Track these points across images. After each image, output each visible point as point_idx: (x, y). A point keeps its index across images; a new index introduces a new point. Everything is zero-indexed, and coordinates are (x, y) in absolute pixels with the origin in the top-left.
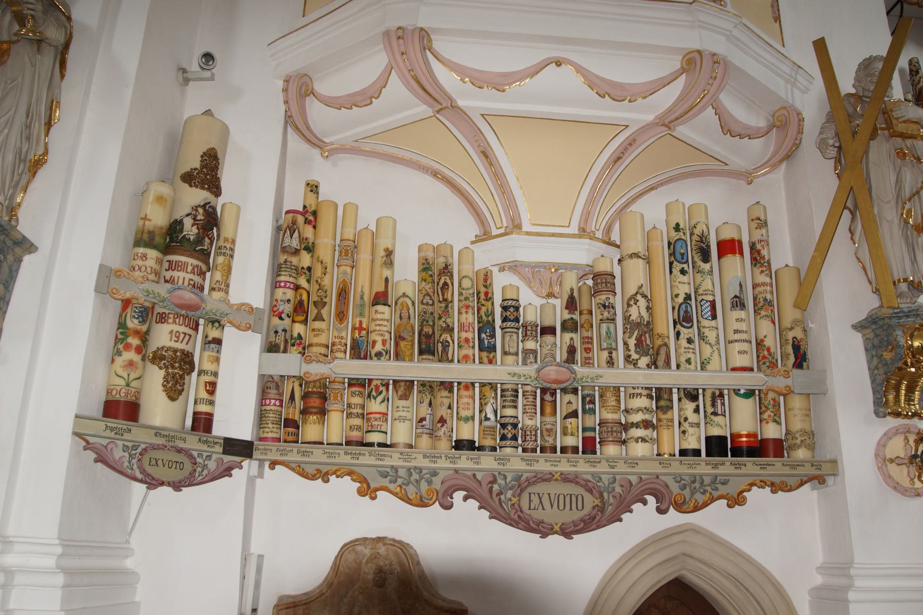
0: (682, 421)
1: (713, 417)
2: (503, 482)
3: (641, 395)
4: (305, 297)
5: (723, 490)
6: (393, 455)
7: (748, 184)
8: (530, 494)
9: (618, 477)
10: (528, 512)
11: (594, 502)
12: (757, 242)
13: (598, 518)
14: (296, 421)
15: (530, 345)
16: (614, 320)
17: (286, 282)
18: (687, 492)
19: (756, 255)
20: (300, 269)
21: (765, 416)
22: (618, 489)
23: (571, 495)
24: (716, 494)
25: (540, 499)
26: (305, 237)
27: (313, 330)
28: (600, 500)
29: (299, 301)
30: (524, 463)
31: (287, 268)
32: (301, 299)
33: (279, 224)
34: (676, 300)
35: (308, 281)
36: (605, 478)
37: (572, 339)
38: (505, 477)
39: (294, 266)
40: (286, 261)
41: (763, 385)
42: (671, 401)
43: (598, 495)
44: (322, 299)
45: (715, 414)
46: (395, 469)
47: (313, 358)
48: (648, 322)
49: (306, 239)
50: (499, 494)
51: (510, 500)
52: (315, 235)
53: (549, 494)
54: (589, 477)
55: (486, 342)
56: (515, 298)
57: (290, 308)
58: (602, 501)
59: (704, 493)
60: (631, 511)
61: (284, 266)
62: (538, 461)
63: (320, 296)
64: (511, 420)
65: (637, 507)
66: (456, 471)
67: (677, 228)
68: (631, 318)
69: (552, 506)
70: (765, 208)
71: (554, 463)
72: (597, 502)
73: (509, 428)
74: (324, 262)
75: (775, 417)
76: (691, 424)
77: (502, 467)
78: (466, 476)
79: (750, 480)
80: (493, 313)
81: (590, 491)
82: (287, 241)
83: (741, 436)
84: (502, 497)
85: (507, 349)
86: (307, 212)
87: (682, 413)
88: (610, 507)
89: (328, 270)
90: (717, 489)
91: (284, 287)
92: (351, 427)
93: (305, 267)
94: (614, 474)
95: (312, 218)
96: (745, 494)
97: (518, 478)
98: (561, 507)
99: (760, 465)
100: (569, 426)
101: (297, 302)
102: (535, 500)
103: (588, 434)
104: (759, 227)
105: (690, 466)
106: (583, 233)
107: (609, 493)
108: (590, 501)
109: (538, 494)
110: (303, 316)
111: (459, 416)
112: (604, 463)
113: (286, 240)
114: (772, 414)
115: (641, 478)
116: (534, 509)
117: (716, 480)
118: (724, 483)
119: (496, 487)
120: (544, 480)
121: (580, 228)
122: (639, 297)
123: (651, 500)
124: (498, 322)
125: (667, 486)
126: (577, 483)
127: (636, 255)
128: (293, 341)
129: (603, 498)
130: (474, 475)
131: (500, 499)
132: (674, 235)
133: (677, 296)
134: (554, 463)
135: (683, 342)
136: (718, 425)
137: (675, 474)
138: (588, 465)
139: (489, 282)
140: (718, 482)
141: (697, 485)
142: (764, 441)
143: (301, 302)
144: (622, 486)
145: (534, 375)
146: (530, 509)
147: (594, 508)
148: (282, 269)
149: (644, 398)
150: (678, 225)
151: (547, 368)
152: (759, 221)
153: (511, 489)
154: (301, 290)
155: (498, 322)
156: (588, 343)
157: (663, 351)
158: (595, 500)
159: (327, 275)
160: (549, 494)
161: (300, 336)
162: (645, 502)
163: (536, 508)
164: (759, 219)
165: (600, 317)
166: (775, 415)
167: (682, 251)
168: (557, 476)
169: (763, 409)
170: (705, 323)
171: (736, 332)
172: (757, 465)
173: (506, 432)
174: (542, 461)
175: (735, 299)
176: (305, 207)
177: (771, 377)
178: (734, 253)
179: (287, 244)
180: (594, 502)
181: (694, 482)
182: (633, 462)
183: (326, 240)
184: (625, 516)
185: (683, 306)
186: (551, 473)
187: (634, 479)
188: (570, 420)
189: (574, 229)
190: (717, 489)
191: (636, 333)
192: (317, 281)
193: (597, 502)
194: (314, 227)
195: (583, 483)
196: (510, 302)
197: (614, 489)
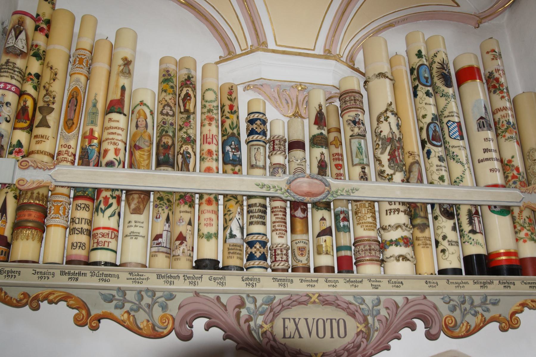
0: (440, 239)
1: (471, 235)
2: (252, 306)
3: (398, 210)
4: (30, 103)
5: (494, 311)
6: (121, 275)
7: (475, 28)
8: (284, 319)
9: (382, 298)
10: (283, 341)
11: (358, 327)
12: (494, 72)
13: (363, 346)
14: (6, 237)
15: (279, 159)
16: (364, 136)
17: (6, 84)
18: (457, 314)
19: (495, 83)
20: (26, 75)
21: (522, 234)
22: (384, 312)
23: (331, 320)
24: (488, 316)
25: (296, 325)
26: (35, 44)
27: (36, 137)
28: (364, 325)
29: (22, 107)
30: (277, 283)
31: (9, 69)
32: (25, 105)
33: (4, 26)
34: (424, 121)
35: (35, 88)
36: (369, 300)
37: (322, 154)
38: (255, 300)
39: (18, 68)
40: (8, 62)
41: (520, 202)
42: (427, 218)
43: (361, 319)
44: (49, 105)
45: (473, 232)
46: (123, 291)
47: (31, 163)
48: (399, 138)
49: (37, 46)
50: (247, 321)
51: (261, 327)
52: (47, 44)
53: (306, 319)
54: (351, 299)
55: (231, 154)
56: (261, 111)
57: (9, 111)
58: (367, 326)
59: (475, 314)
60: (399, 338)
61: (4, 67)
62: (292, 281)
63: (47, 102)
64: (260, 238)
65: (405, 332)
66: (197, 294)
67: (419, 54)
68: (382, 134)
69: (310, 333)
70: (497, 42)
71: (311, 284)
72: (361, 327)
73: (258, 246)
74: (53, 68)
75: (533, 236)
76: (451, 243)
77: (250, 288)
78: (208, 299)
79: (521, 300)
80: (238, 126)
81: (353, 315)
82: (11, 42)
83: (499, 255)
84: (252, 324)
85: (254, 162)
86: (39, 20)
87: (439, 232)
88: (376, 333)
89: (57, 76)
90: (488, 310)
91: (4, 88)
92: (73, 244)
93: (33, 73)
94: (378, 295)
95: (45, 26)
96: (517, 315)
97: (269, 301)
98: (321, 334)
99: (529, 283)
100: (324, 244)
101: (20, 107)
103: (343, 253)
104: (494, 58)
105: (458, 285)
106: (328, 55)
107: (374, 317)
109: (294, 319)
110: (26, 123)
111: (201, 233)
112: (366, 282)
113: (10, 41)
114: (529, 233)
115: (407, 299)
116: (290, 337)
117: (486, 300)
118: (495, 304)
119: (244, 312)
120: (300, 303)
121: (325, 51)
122: (389, 114)
123: (419, 324)
124: (244, 136)
125: (436, 307)
126: (338, 306)
127: (382, 75)
128: (11, 149)
129: (368, 323)
130: (218, 298)
131: (249, 326)
132: (416, 62)
133: (424, 116)
134: (311, 284)
135: (434, 160)
136: (477, 243)
137: (443, 294)
138: (348, 285)
139: (233, 96)
140: (488, 302)
141: (467, 306)
142: (523, 261)
143: (25, 109)
144: (387, 308)
145: (284, 186)
147: (358, 334)
148: (2, 70)
149: (402, 214)
150: (420, 52)
151: (298, 180)
152: (494, 53)
153: (262, 314)
154: (26, 96)
155: (244, 136)
156: (339, 159)
157: (415, 168)
158: (359, 325)
159: (56, 80)
160: (306, 319)
161: (19, 144)
162: (413, 328)
163: (292, 336)
164: (494, 51)
165: (351, 133)
166: (532, 234)
167: (426, 75)
168: (314, 298)
169: (519, 228)
170: (453, 142)
171: (486, 151)
172: (525, 283)
173: (254, 250)
174: (296, 280)
175: (481, 120)
176: (38, 15)
177: (526, 193)
178: (474, 79)
179: (11, 45)
180: (358, 327)
181: (463, 302)
182: (397, 281)
183: (58, 47)
184: (393, 343)
185: (432, 126)
186: (307, 295)
187: (400, 301)
188: (324, 238)
189: (319, 51)
190: (488, 310)
191: (389, 148)
192: (44, 87)
193: (361, 327)
194: (47, 36)
195: (344, 305)
196: (256, 115)
197: (379, 312)
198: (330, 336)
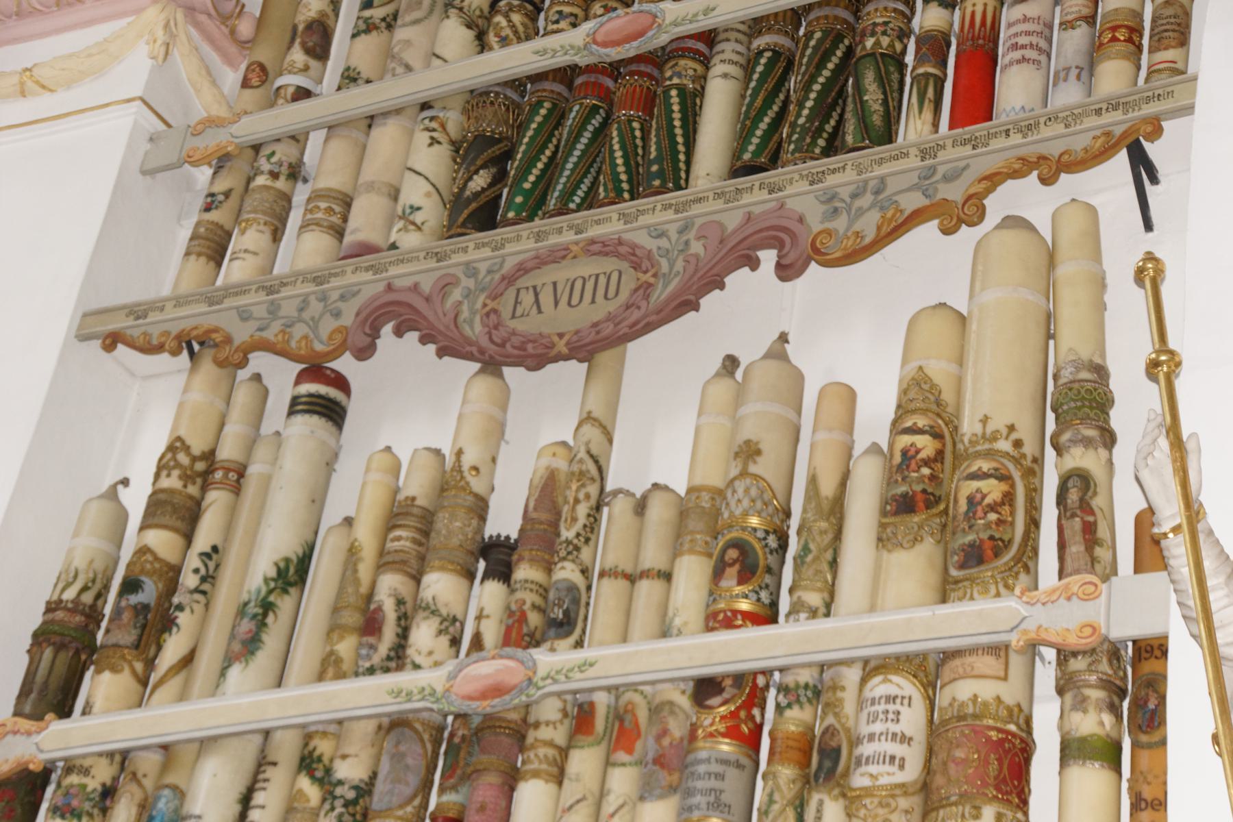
11: (638, 279)
23: (597, 276)
53: (555, 284)
69: (556, 303)
98: (575, 301)
102: (527, 299)
108: (630, 281)
116: (522, 316)
146: (513, 317)
160: (555, 284)
180: (638, 279)
198: (590, 300)
